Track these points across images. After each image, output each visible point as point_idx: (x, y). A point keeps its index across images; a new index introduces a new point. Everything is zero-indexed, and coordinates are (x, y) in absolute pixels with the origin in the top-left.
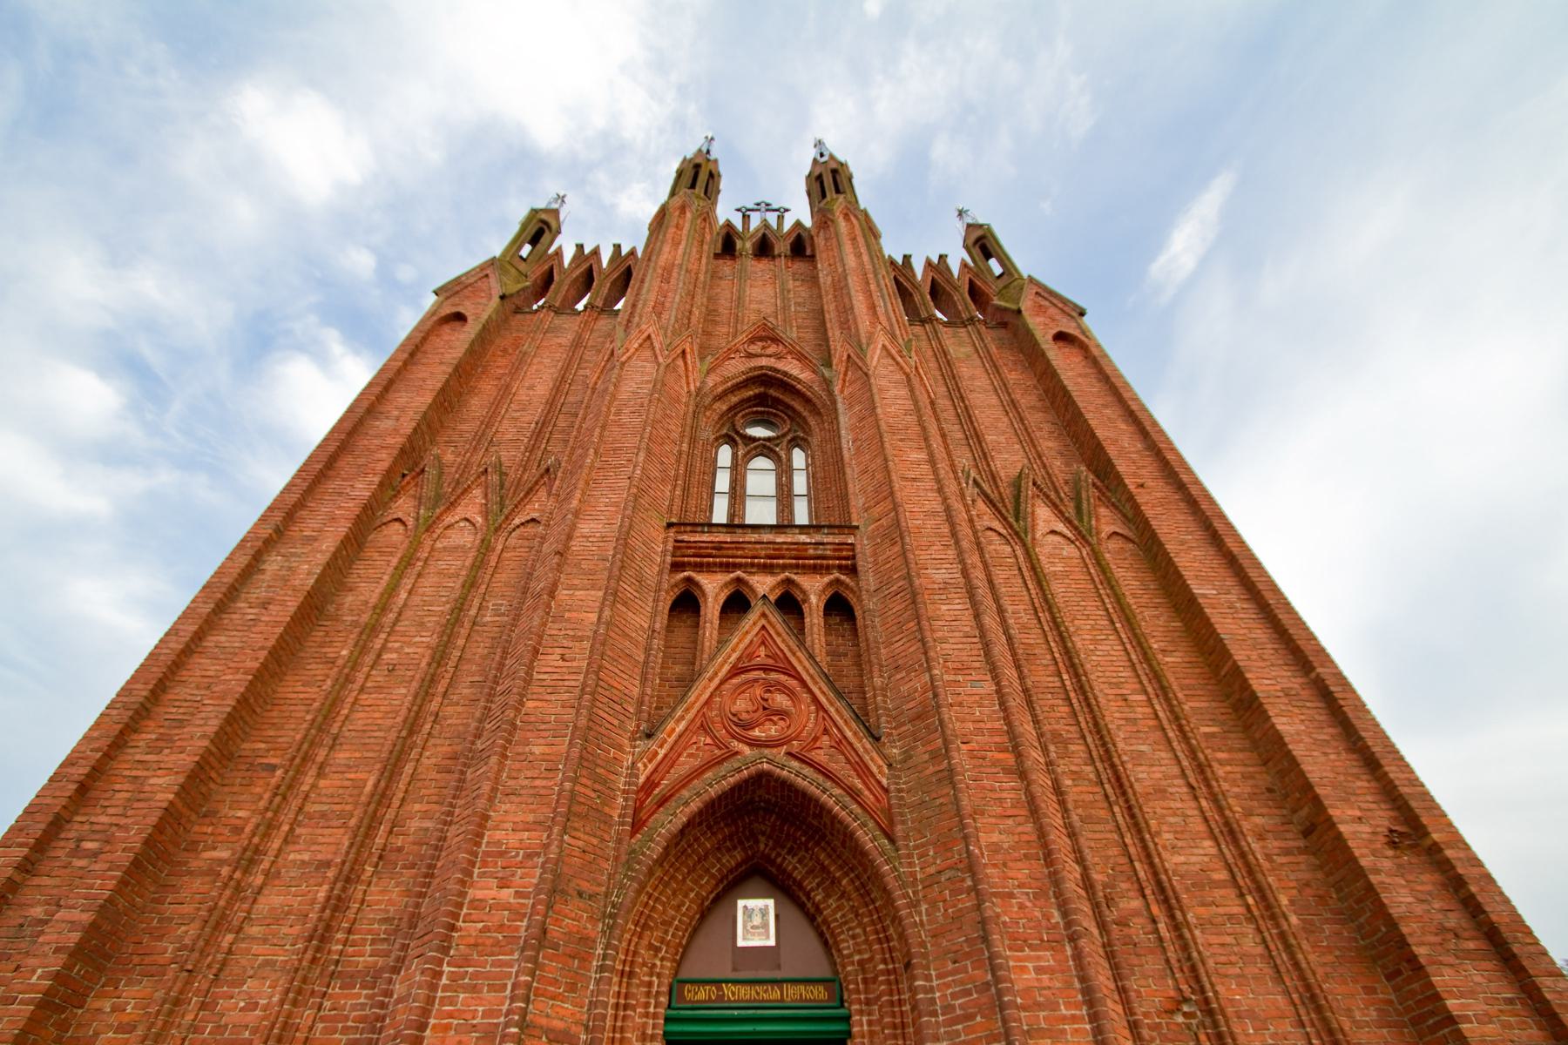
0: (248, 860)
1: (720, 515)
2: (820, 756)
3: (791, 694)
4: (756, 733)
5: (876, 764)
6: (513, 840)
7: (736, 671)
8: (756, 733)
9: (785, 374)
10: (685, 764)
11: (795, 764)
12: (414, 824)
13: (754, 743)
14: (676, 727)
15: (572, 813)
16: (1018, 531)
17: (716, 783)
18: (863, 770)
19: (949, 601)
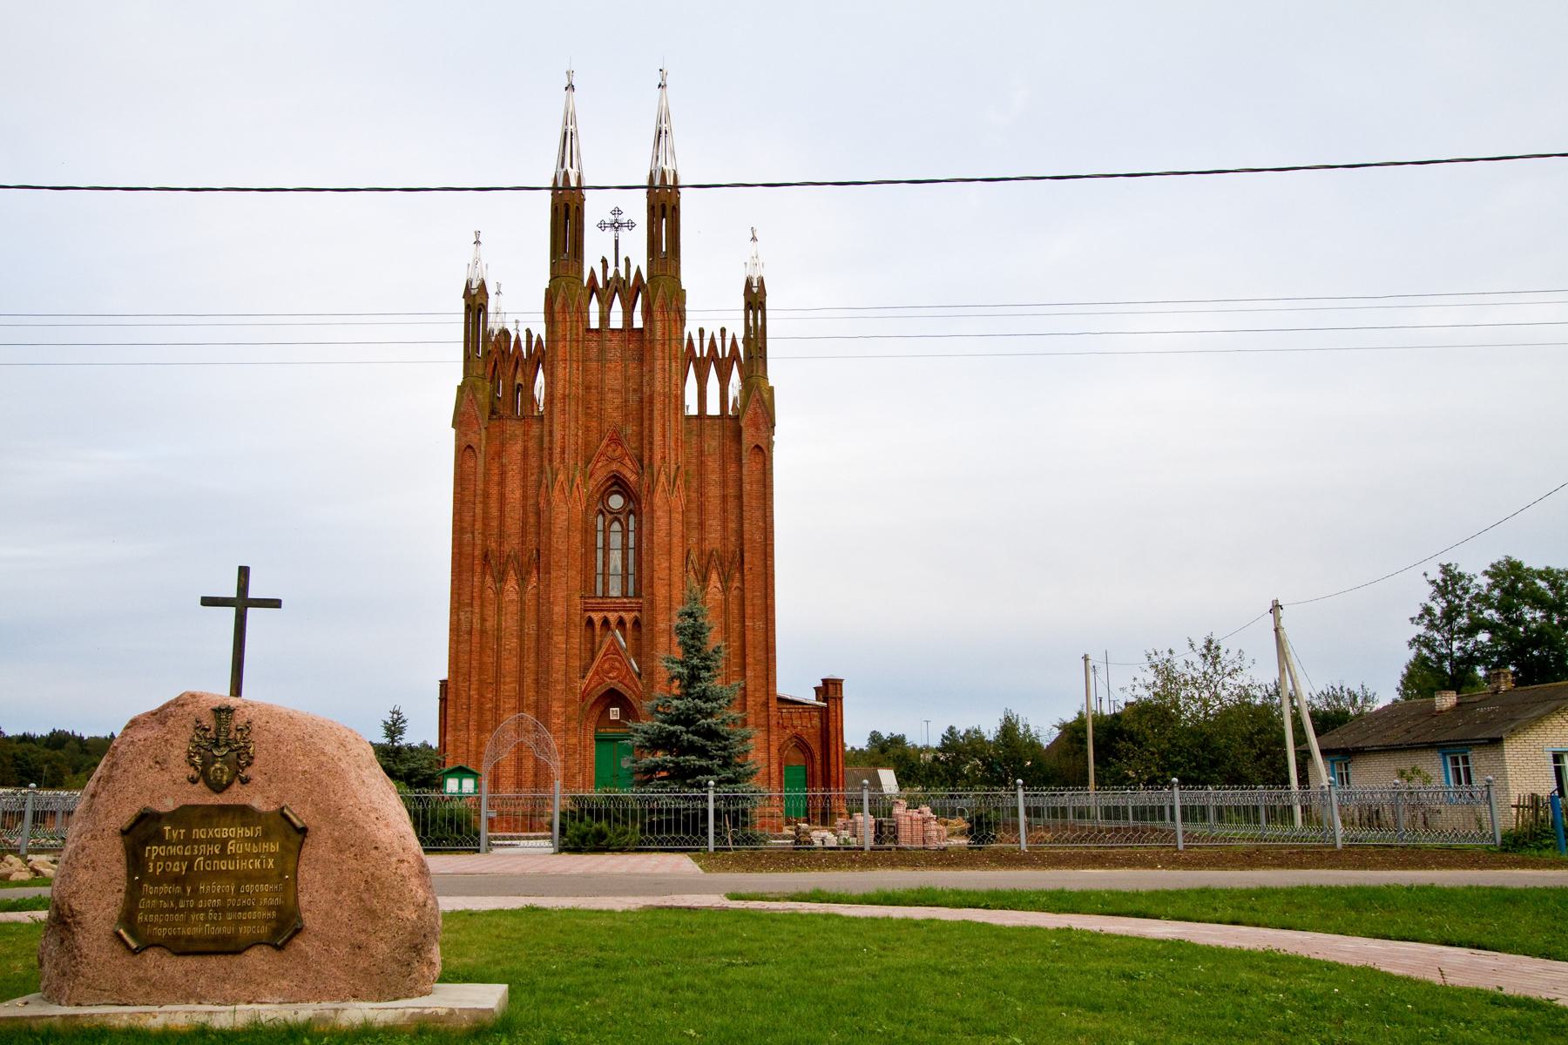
0: (497, 708)
1: (599, 593)
2: (626, 681)
3: (620, 663)
4: (611, 675)
5: (639, 684)
6: (557, 710)
7: (605, 655)
8: (611, 675)
9: (624, 476)
10: (592, 686)
11: (620, 685)
12: (531, 698)
13: (610, 678)
14: (590, 674)
15: (567, 703)
16: (704, 579)
17: (601, 690)
18: (637, 686)
19: (663, 637)
